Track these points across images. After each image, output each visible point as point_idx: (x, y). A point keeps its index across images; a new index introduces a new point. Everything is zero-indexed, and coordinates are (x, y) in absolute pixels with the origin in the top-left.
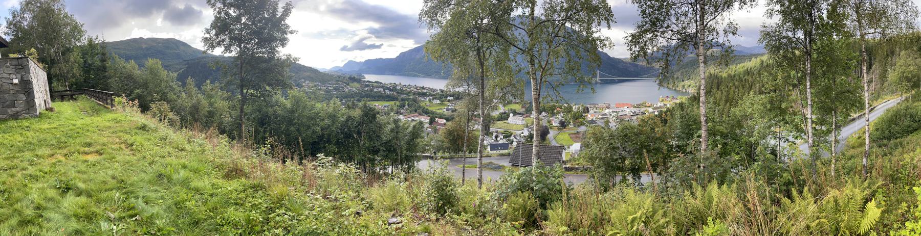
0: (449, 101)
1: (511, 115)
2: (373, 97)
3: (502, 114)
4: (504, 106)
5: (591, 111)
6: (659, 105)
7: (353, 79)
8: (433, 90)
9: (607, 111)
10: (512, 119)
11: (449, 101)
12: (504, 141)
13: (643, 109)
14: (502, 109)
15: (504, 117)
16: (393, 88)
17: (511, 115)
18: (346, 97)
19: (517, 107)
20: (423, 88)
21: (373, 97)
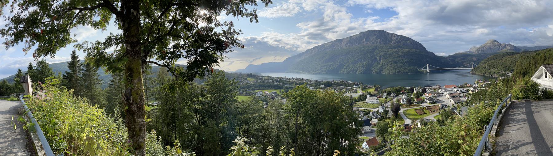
0: (322, 88)
1: (368, 96)
2: (264, 86)
3: (361, 96)
4: (363, 89)
5: (428, 92)
6: (477, 85)
7: (250, 76)
8: (310, 81)
9: (440, 90)
10: (369, 100)
11: (322, 88)
12: (365, 118)
13: (466, 89)
14: (360, 92)
15: (363, 98)
16: (280, 80)
17: (368, 96)
18: (244, 88)
19: (372, 91)
20: (303, 79)
21: (264, 86)
